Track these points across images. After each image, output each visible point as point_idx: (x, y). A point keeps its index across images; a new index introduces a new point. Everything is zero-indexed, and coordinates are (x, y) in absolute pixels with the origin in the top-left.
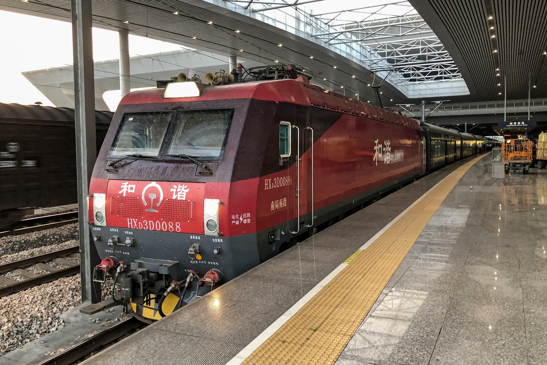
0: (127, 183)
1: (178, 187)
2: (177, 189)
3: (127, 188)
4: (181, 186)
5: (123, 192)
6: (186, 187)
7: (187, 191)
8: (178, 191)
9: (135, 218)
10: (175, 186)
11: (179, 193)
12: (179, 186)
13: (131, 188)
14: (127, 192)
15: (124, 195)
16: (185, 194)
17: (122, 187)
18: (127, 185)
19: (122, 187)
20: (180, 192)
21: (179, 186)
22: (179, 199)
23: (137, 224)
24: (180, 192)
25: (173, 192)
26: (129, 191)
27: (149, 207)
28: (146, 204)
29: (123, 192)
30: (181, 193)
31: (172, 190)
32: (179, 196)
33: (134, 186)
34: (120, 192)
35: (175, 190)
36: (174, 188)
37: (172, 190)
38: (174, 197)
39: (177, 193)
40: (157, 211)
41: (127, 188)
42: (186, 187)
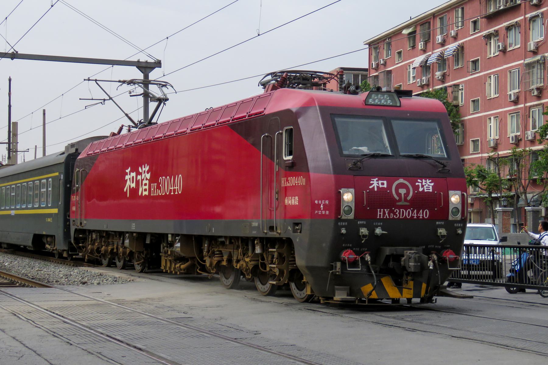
0: (377, 179)
2: (422, 183)
3: (378, 184)
4: (426, 180)
6: (430, 181)
7: (432, 184)
8: (424, 184)
10: (419, 181)
11: (425, 186)
12: (424, 180)
14: (378, 187)
15: (376, 189)
16: (431, 187)
18: (377, 181)
21: (424, 180)
22: (426, 191)
24: (427, 186)
26: (381, 186)
30: (427, 186)
31: (417, 184)
32: (425, 188)
33: (385, 182)
35: (420, 184)
36: (419, 182)
37: (417, 184)
38: (421, 189)
39: (423, 186)
41: (378, 184)
42: (430, 181)
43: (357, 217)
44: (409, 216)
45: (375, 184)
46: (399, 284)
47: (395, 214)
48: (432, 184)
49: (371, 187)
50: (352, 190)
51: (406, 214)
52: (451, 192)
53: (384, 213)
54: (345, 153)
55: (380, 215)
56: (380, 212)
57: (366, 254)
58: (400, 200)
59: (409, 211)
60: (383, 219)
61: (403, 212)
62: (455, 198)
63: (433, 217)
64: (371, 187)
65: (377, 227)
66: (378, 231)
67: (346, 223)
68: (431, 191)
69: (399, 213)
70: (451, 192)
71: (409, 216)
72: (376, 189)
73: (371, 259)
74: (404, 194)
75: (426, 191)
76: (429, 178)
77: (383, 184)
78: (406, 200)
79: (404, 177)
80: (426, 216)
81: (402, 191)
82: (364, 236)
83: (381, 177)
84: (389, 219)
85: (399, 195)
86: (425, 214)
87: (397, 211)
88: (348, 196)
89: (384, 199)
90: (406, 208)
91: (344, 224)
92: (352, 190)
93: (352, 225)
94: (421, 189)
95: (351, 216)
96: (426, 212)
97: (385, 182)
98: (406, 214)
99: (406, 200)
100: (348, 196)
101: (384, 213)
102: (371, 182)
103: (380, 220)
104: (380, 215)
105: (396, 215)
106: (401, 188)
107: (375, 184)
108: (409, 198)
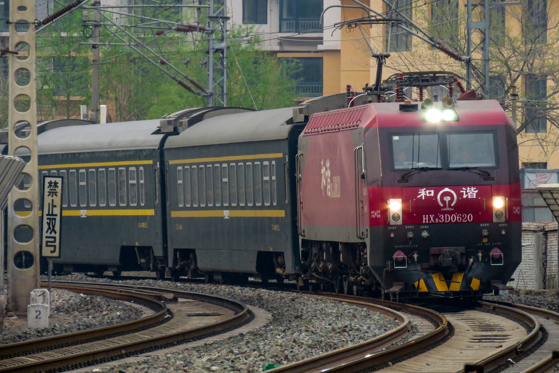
1: (467, 188)
2: (466, 191)
4: (470, 188)
7: (477, 191)
9: (432, 214)
10: (464, 189)
12: (468, 188)
13: (430, 193)
14: (425, 196)
16: (475, 194)
17: (419, 192)
19: (419, 192)
21: (468, 188)
22: (469, 197)
23: (434, 219)
24: (471, 193)
25: (463, 193)
30: (471, 193)
31: (461, 191)
34: (418, 197)
35: (464, 192)
37: (461, 191)
38: (465, 196)
39: (467, 193)
40: (453, 209)
43: (405, 222)
44: (454, 219)
45: (423, 193)
46: (448, 280)
47: (439, 219)
48: (477, 191)
51: (451, 218)
54: (396, 167)
55: (426, 221)
56: (426, 217)
57: (414, 254)
58: (445, 206)
59: (454, 217)
62: (499, 203)
63: (477, 219)
65: (424, 230)
66: (425, 234)
68: (475, 197)
69: (444, 218)
71: (454, 219)
73: (418, 258)
74: (449, 201)
75: (469, 197)
76: (474, 185)
78: (450, 206)
80: (470, 219)
82: (411, 239)
84: (435, 223)
85: (444, 202)
86: (470, 217)
89: (431, 206)
90: (450, 213)
91: (393, 228)
94: (465, 196)
95: (400, 222)
96: (470, 216)
98: (451, 218)
100: (395, 206)
103: (426, 224)
104: (426, 221)
105: (442, 220)
106: (447, 195)
107: (423, 193)
108: (452, 205)
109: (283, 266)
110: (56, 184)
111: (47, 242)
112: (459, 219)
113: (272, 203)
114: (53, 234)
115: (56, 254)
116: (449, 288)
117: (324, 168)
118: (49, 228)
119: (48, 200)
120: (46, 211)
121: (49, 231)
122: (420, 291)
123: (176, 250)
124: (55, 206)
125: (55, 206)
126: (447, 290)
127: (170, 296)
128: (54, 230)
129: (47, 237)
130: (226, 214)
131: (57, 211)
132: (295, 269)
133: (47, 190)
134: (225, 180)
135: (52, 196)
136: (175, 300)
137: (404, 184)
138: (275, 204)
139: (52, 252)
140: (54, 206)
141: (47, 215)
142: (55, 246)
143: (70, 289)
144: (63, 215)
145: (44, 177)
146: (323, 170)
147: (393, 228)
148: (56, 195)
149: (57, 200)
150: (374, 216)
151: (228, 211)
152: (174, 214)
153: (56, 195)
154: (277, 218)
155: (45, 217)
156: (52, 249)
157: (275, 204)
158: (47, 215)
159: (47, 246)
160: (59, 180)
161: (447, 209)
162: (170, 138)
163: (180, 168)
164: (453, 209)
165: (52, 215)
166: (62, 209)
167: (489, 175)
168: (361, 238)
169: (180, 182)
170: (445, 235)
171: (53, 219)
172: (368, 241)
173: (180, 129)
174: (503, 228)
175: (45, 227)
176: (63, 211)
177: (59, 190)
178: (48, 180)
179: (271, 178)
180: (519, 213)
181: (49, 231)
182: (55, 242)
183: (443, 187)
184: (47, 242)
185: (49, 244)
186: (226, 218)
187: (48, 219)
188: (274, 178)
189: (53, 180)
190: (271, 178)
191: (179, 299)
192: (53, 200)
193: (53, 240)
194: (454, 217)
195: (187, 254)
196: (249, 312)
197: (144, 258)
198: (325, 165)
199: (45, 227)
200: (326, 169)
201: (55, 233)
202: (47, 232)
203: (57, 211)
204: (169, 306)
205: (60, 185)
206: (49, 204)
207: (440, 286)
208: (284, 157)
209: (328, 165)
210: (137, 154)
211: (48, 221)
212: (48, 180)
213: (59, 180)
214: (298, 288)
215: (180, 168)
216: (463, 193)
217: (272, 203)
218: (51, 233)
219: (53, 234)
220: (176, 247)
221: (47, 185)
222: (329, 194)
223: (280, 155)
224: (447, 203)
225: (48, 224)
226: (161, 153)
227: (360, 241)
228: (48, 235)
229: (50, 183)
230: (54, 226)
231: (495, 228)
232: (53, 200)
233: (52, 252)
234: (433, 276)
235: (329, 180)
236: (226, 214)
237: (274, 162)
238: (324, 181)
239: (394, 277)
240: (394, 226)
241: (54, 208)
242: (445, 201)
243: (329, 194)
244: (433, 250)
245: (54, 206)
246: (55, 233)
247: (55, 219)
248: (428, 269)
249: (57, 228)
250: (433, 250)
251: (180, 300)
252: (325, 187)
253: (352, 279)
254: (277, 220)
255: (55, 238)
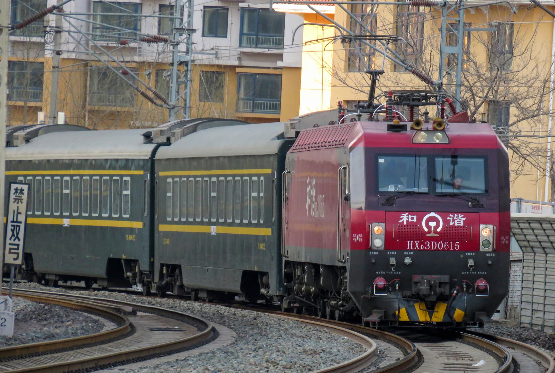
5: (403, 222)
7: (464, 219)
8: (455, 218)
10: (451, 215)
12: (456, 215)
13: (412, 218)
14: (407, 221)
15: (405, 223)
20: (458, 220)
21: (456, 215)
22: (456, 225)
24: (458, 220)
25: (450, 220)
26: (410, 220)
27: (429, 232)
28: (426, 230)
29: (403, 222)
30: (458, 220)
31: (448, 218)
32: (456, 223)
35: (451, 219)
36: (450, 217)
37: (448, 218)
38: (451, 224)
39: (454, 221)
40: (438, 235)
41: (408, 218)
45: (405, 218)
48: (464, 219)
49: (400, 221)
50: (383, 224)
52: (482, 226)
53: (414, 245)
55: (410, 247)
56: (410, 243)
58: (429, 232)
60: (413, 250)
61: (434, 244)
64: (400, 221)
66: (408, 260)
67: (377, 253)
68: (462, 225)
69: (430, 245)
70: (482, 226)
72: (405, 223)
74: (434, 227)
75: (456, 225)
76: (461, 213)
77: (412, 218)
79: (436, 212)
81: (433, 224)
83: (411, 212)
84: (420, 250)
85: (429, 227)
87: (427, 243)
88: (378, 229)
90: (437, 240)
91: (375, 253)
92: (383, 224)
93: (383, 254)
94: (451, 224)
97: (415, 217)
99: (435, 232)
100: (378, 229)
101: (414, 245)
102: (401, 217)
104: (410, 247)
105: (428, 247)
106: (433, 223)
107: (405, 218)
109: (267, 286)
110: (22, 190)
111: (10, 249)
112: (447, 247)
113: (259, 221)
114: (17, 242)
115: (19, 262)
116: (431, 318)
117: (310, 186)
118: (13, 235)
119: (13, 206)
120: (10, 218)
121: (13, 238)
122: (400, 319)
123: (162, 266)
124: (20, 213)
125: (20, 213)
126: (428, 319)
127: (129, 309)
128: (17, 237)
129: (10, 244)
130: (213, 230)
131: (21, 218)
132: (279, 290)
133: (12, 196)
134: (214, 194)
135: (18, 203)
136: (134, 313)
137: (389, 208)
138: (262, 222)
139: (15, 259)
140: (19, 213)
141: (12, 222)
142: (18, 254)
143: (25, 297)
144: (27, 222)
145: (11, 183)
146: (309, 189)
147: (375, 253)
148: (22, 203)
149: (23, 207)
150: (355, 240)
151: (215, 227)
152: (162, 228)
153: (22, 203)
154: (264, 237)
155: (9, 224)
156: (15, 256)
157: (262, 222)
158: (12, 222)
159: (10, 253)
160: (25, 187)
161: (432, 234)
162: (161, 149)
163: (170, 180)
164: (438, 235)
165: (17, 222)
166: (27, 216)
167: (478, 202)
168: (342, 262)
169: (169, 194)
170: (426, 263)
171: (17, 226)
172: (348, 265)
173: (172, 139)
174: (490, 258)
175: (9, 233)
176: (28, 219)
177: (25, 197)
178: (14, 186)
179: (259, 194)
180: (507, 242)
181: (13, 238)
182: (18, 249)
183: (430, 212)
184: (10, 249)
185: (12, 251)
186: (213, 234)
187: (12, 226)
188: (262, 194)
189: (19, 186)
190: (259, 194)
191: (138, 312)
192: (18, 207)
193: (16, 247)
194: (441, 244)
195: (174, 270)
196: (213, 329)
197: (131, 271)
198: (310, 183)
199: (9, 233)
200: (312, 188)
201: (19, 240)
202: (10, 239)
203: (21, 218)
204: (132, 319)
205: (26, 192)
206: (14, 211)
207: (422, 316)
208: (273, 174)
209: (313, 183)
210: (127, 164)
211: (13, 228)
212: (14, 186)
213: (25, 187)
214: (283, 310)
215: (170, 180)
216: (450, 220)
217: (259, 221)
218: (14, 240)
219: (17, 242)
220: (163, 262)
221: (12, 191)
222: (313, 214)
223: (269, 171)
224: (432, 229)
225: (13, 231)
226: (151, 164)
227: (341, 264)
228: (12, 242)
229: (16, 190)
230: (18, 234)
231: (481, 258)
232: (18, 207)
233: (15, 259)
234: (415, 304)
235: (314, 199)
236: (213, 230)
237: (262, 178)
238: (309, 200)
239: (373, 303)
240: (376, 251)
241: (19, 215)
242: (431, 227)
243: (313, 214)
244: (417, 278)
245: (19, 213)
246: (19, 240)
247: (19, 226)
248: (409, 297)
249: (21, 235)
250: (417, 278)
251: (139, 313)
252: (310, 207)
253: (333, 302)
254: (263, 239)
255: (18, 245)
